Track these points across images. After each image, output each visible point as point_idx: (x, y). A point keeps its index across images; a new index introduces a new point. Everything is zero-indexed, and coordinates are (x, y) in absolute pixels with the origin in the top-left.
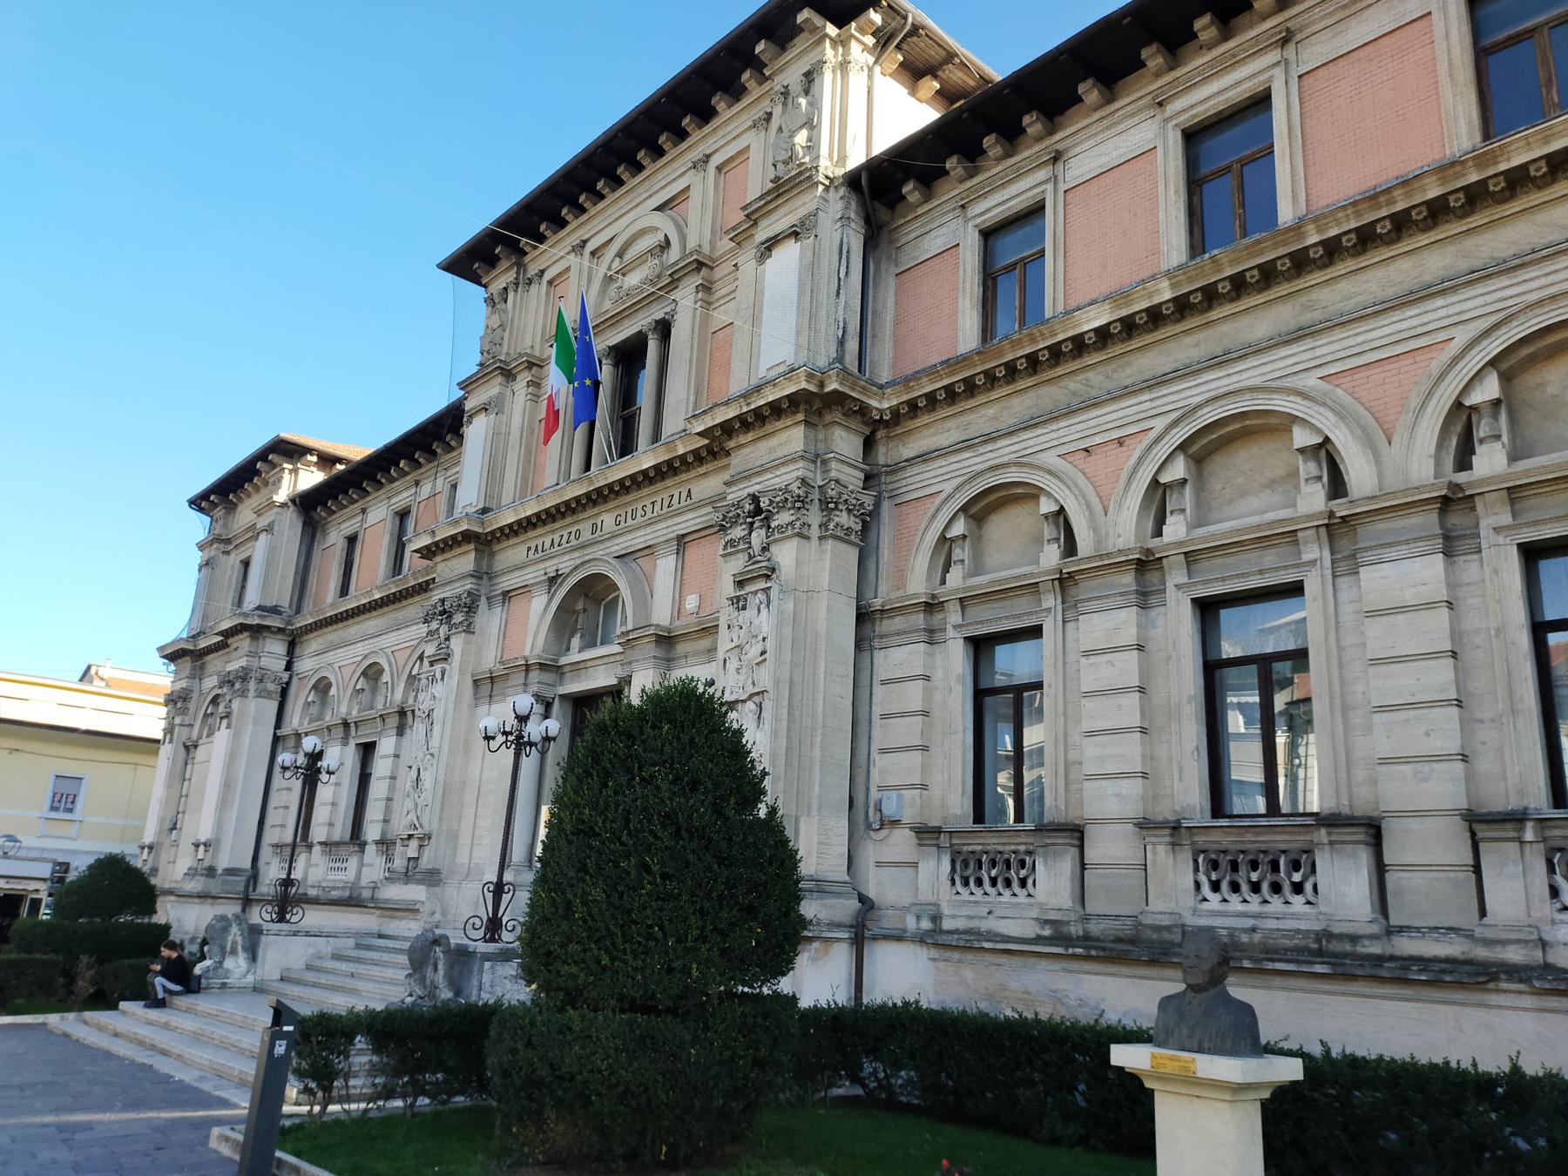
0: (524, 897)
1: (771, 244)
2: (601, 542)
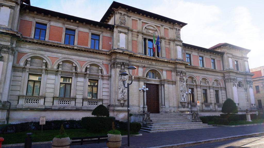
0: (147, 109)
1: (178, 45)
2: (157, 66)
